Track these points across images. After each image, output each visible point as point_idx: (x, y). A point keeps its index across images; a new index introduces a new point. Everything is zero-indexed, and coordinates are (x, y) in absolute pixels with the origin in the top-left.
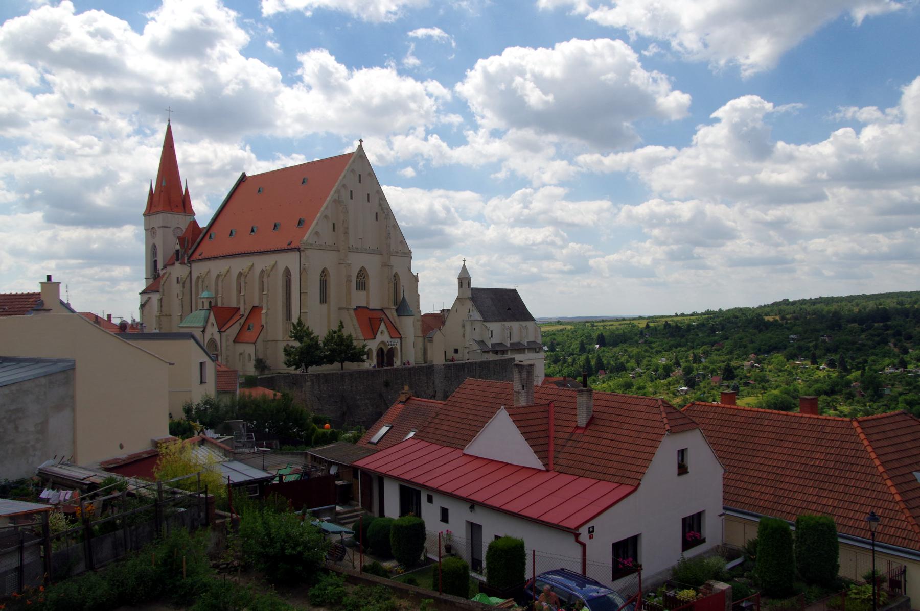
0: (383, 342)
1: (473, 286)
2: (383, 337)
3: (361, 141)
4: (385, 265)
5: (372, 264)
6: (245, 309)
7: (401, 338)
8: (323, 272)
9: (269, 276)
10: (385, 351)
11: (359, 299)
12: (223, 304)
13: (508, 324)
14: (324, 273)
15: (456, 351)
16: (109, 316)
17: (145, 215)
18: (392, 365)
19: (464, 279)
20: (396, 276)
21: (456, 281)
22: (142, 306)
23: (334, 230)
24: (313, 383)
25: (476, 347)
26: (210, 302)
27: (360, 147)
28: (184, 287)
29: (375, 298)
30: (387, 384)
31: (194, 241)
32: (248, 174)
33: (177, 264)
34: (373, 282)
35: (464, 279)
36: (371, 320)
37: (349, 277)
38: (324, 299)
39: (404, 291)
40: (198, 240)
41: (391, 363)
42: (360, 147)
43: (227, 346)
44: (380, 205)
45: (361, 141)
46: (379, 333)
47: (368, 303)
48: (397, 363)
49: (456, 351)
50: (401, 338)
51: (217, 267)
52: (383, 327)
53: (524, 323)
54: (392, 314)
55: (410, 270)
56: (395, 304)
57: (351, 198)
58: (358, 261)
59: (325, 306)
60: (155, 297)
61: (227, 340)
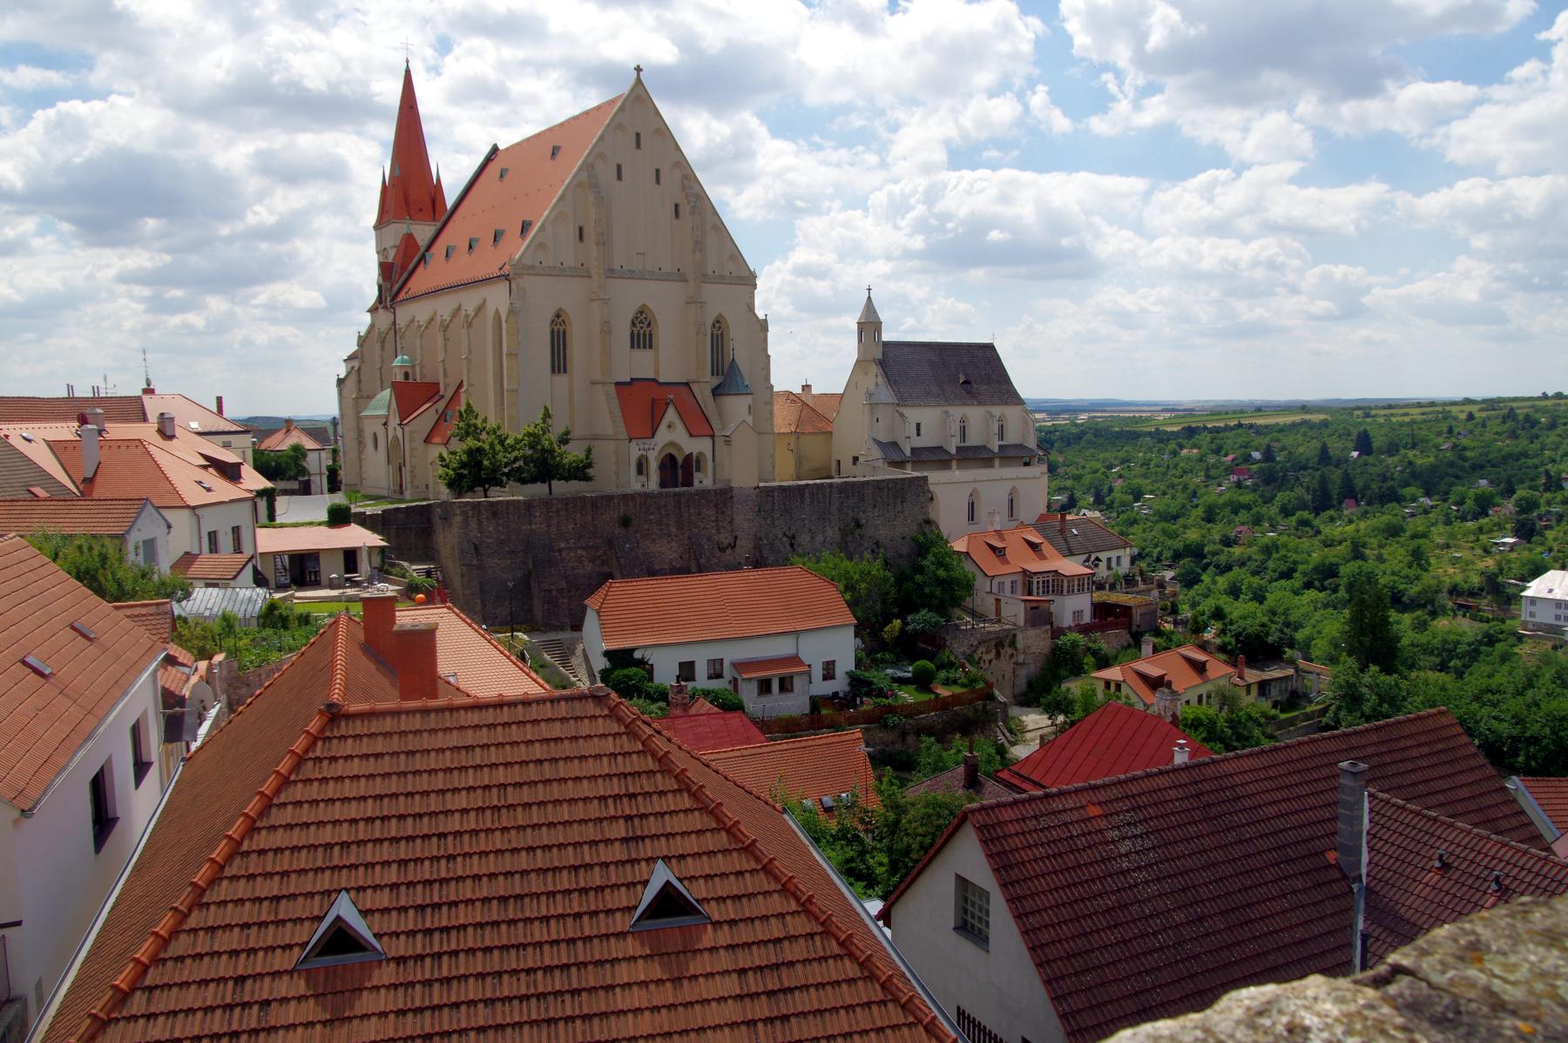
0: (672, 444)
1: (886, 337)
2: (673, 434)
4: (694, 301)
5: (664, 301)
6: (446, 386)
7: (713, 436)
8: (558, 316)
9: (470, 325)
10: (680, 460)
12: (423, 376)
13: (957, 412)
15: (856, 459)
16: (219, 400)
17: (376, 228)
18: (690, 484)
19: (869, 325)
20: (718, 323)
21: (855, 327)
22: (340, 382)
23: (581, 238)
24: (466, 519)
25: (877, 453)
26: (406, 375)
27: (639, 81)
28: (383, 348)
29: (671, 360)
30: (625, 522)
31: (403, 268)
32: (501, 147)
33: (381, 311)
34: (666, 332)
35: (869, 325)
36: (644, 402)
37: (606, 329)
38: (559, 363)
39: (739, 352)
40: (411, 267)
41: (688, 482)
42: (639, 81)
43: (412, 450)
44: (684, 188)
46: (663, 427)
47: (657, 373)
48: (704, 480)
49: (856, 459)
50: (713, 436)
51: (420, 312)
52: (671, 415)
53: (997, 410)
54: (703, 393)
56: (715, 371)
57: (619, 177)
58: (629, 297)
59: (561, 379)
60: (356, 364)
61: (412, 440)
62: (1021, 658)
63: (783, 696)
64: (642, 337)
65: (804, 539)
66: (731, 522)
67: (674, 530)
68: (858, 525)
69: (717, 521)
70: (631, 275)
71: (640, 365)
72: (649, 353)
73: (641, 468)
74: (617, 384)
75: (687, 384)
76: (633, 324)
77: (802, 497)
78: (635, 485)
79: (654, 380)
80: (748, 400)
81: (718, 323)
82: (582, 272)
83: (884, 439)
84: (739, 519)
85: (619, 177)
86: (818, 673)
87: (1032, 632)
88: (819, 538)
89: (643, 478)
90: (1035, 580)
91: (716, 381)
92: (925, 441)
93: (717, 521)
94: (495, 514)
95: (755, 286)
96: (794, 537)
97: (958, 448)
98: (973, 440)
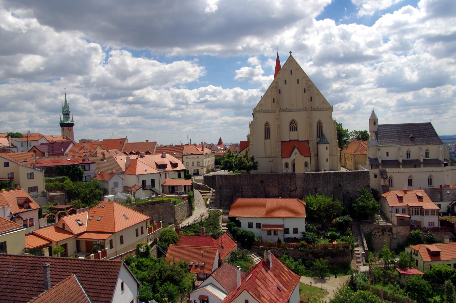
3: (291, 52)
4: (310, 117)
8: (267, 124)
11: (288, 136)
14: (267, 124)
20: (319, 123)
24: (219, 179)
27: (291, 56)
30: (262, 182)
34: (300, 127)
35: (373, 120)
42: (291, 56)
45: (291, 52)
52: (296, 150)
55: (331, 117)
57: (286, 83)
59: (268, 141)
62: (395, 236)
63: (275, 236)
64: (293, 127)
65: (320, 189)
66: (295, 183)
67: (276, 185)
68: (340, 186)
69: (290, 183)
70: (290, 111)
71: (294, 136)
72: (296, 132)
73: (287, 165)
74: (282, 142)
75: (308, 141)
76: (291, 124)
77: (319, 177)
78: (284, 171)
79: (297, 140)
80: (327, 145)
81: (319, 123)
82: (273, 111)
83: (372, 157)
84: (298, 182)
85: (286, 83)
86: (291, 231)
87: (400, 228)
88: (326, 189)
89: (287, 169)
90: (411, 209)
91: (318, 140)
92: (390, 158)
93: (290, 183)
94: (226, 178)
95: (332, 110)
96: (316, 189)
97: (424, 160)
98: (413, 157)
